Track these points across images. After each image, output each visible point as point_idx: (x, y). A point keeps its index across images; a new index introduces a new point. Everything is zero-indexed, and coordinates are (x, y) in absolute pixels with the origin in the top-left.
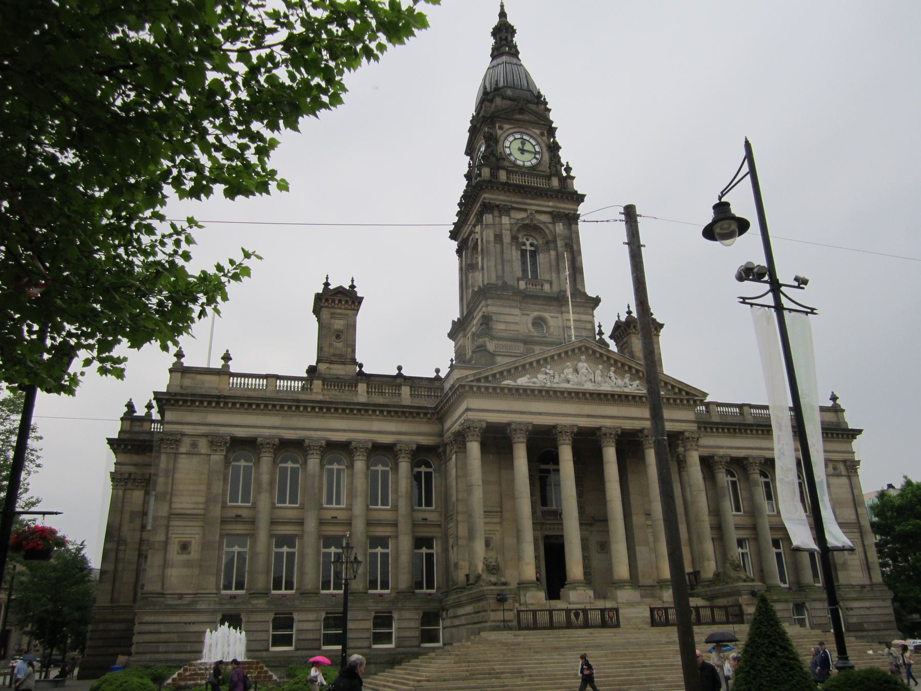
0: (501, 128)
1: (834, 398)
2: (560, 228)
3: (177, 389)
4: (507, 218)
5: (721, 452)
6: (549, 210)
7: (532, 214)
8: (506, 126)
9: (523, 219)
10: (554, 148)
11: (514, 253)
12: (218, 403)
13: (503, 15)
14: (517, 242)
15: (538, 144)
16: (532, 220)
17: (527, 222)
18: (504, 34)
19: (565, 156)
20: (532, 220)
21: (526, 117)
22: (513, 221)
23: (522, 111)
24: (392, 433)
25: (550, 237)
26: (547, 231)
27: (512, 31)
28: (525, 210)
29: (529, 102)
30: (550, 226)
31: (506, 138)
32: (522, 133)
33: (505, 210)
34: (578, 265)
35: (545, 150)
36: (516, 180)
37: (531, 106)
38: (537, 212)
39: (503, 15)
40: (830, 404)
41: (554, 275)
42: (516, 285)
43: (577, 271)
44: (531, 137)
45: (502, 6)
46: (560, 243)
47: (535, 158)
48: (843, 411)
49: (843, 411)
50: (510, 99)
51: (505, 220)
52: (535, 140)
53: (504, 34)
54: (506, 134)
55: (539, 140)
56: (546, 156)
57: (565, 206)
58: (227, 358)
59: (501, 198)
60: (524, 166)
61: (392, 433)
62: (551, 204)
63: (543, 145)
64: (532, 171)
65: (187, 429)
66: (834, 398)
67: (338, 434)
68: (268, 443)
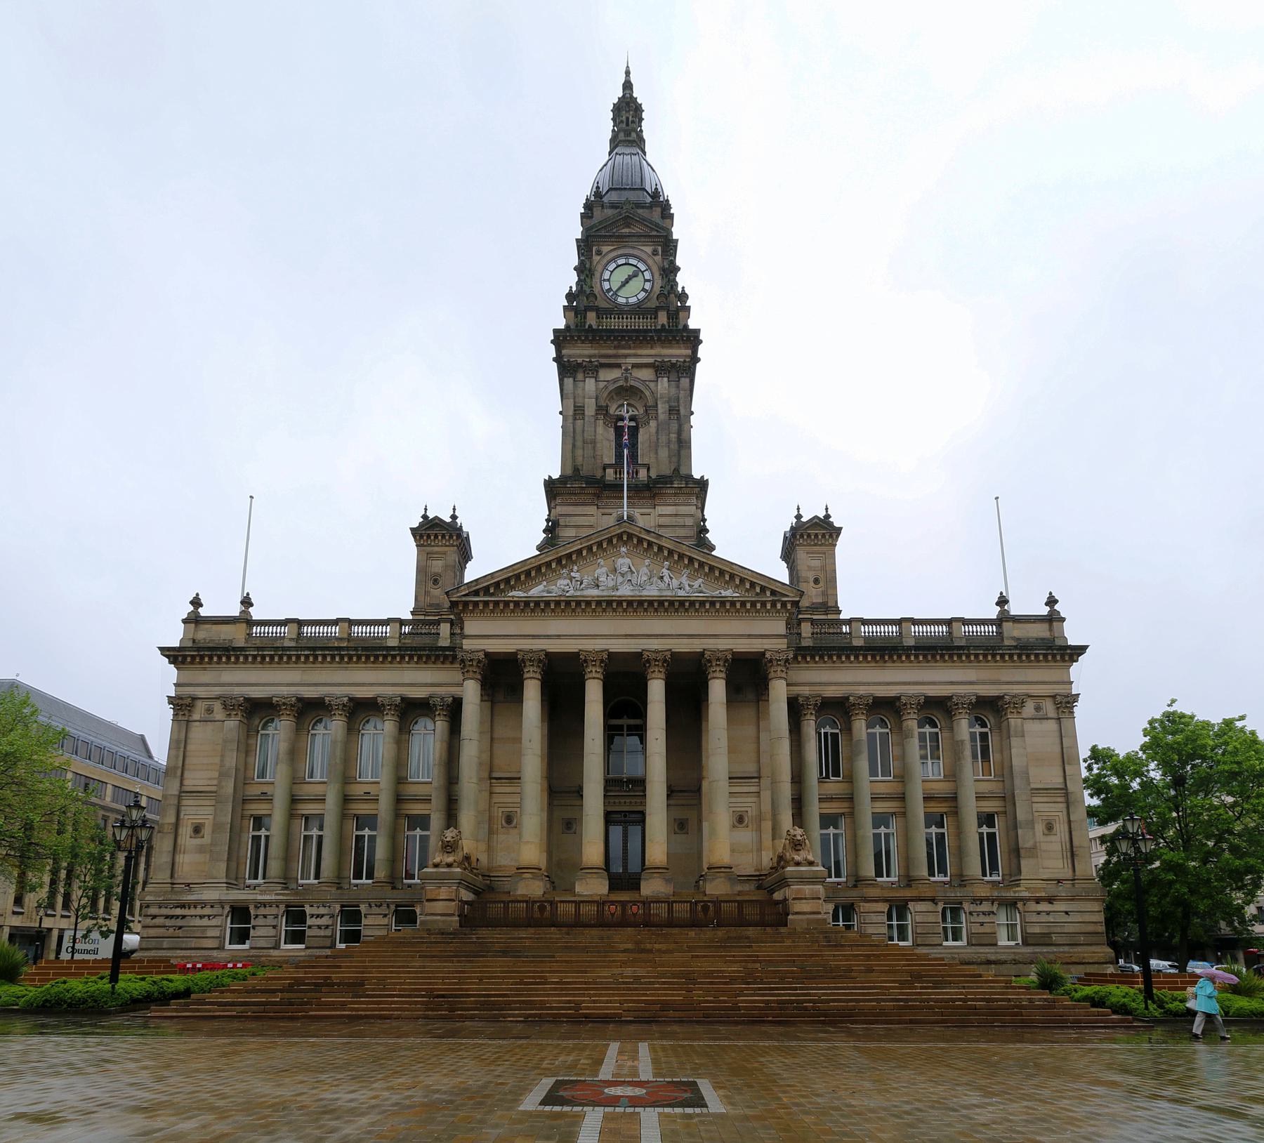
0: (599, 253)
1: (1052, 601)
2: (663, 385)
3: (190, 644)
4: (593, 380)
5: (862, 691)
6: (651, 360)
7: (626, 370)
8: (605, 249)
9: (615, 381)
10: (670, 270)
11: (600, 430)
12: (228, 658)
13: (628, 86)
14: (607, 414)
15: (649, 268)
16: (626, 379)
17: (621, 383)
18: (628, 115)
19: (682, 280)
20: (626, 379)
21: (636, 230)
22: (602, 385)
23: (627, 221)
24: (426, 685)
25: (650, 403)
26: (647, 393)
27: (638, 109)
28: (618, 366)
29: (639, 205)
30: (652, 385)
31: (605, 268)
32: (627, 256)
33: (592, 369)
34: (684, 436)
35: (657, 275)
36: (614, 323)
37: (640, 211)
38: (635, 366)
39: (628, 86)
40: (1045, 611)
41: (652, 455)
42: (599, 474)
43: (683, 445)
44: (640, 259)
45: (628, 73)
46: (662, 408)
47: (644, 290)
48: (1063, 620)
49: (1063, 620)
50: (613, 206)
51: (590, 385)
52: (645, 262)
53: (628, 115)
54: (605, 261)
55: (650, 262)
56: (659, 283)
57: (677, 353)
58: (247, 602)
59: (586, 352)
60: (627, 304)
61: (426, 685)
62: (653, 352)
63: (655, 269)
64: (639, 310)
65: (200, 692)
66: (1052, 601)
67: (365, 688)
68: (284, 704)
